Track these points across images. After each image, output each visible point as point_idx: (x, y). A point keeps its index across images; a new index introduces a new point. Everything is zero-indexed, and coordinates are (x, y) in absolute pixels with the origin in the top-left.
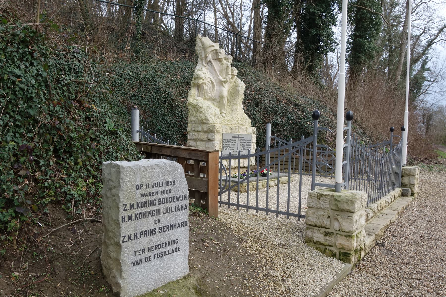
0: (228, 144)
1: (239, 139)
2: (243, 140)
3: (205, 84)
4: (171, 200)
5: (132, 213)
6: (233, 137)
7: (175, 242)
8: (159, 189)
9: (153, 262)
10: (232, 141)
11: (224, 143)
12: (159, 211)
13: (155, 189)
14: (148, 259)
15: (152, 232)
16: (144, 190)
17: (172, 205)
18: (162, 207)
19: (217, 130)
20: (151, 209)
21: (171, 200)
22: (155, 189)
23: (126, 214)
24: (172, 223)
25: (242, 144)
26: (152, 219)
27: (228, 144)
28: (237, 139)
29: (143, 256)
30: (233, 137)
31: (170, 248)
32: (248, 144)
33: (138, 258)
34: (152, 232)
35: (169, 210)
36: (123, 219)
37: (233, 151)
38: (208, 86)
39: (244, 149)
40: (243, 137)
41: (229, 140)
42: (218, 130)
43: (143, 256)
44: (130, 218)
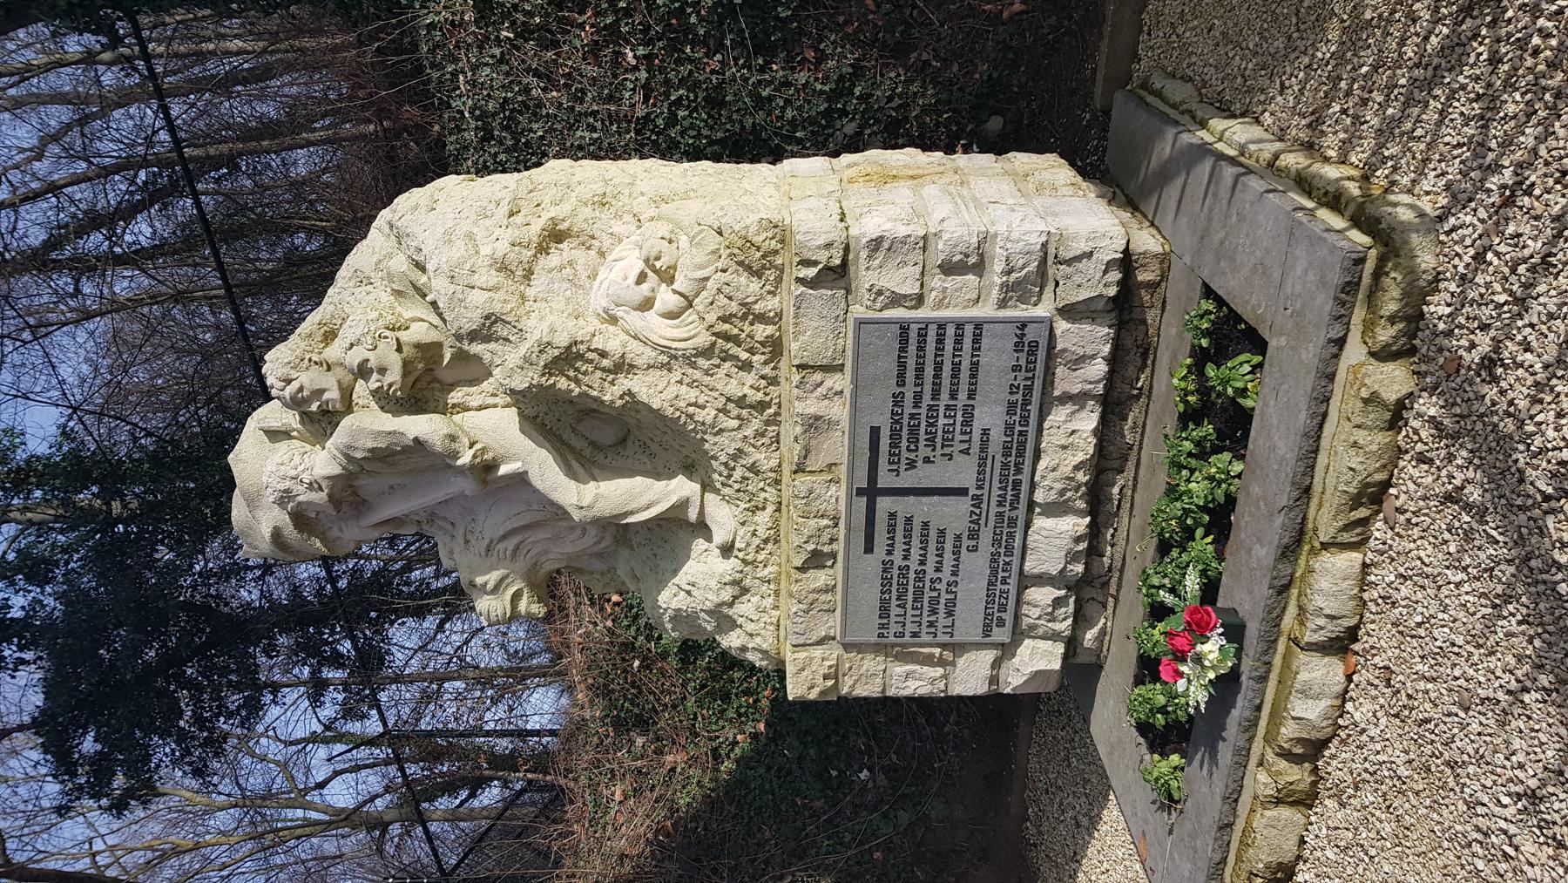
0: (918, 598)
1: (882, 483)
6: (869, 549)
11: (910, 628)
25: (924, 451)
27: (918, 598)
28: (884, 504)
30: (869, 549)
32: (929, 371)
37: (966, 542)
38: (546, 552)
39: (967, 422)
40: (875, 432)
41: (886, 583)
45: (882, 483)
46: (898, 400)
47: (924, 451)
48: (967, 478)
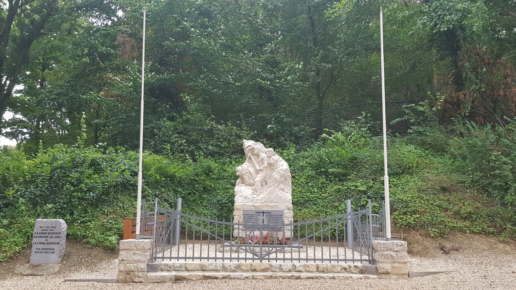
2: (271, 215)
3: (244, 174)
4: (53, 233)
5: (37, 235)
7: (53, 249)
8: (49, 229)
9: (43, 254)
10: (255, 216)
12: (48, 237)
13: (47, 229)
14: (41, 252)
15: (44, 243)
16: (43, 228)
17: (54, 236)
18: (49, 236)
19: (236, 208)
20: (44, 235)
21: (53, 233)
22: (47, 229)
23: (35, 235)
24: (53, 242)
26: (45, 239)
29: (39, 251)
31: (51, 251)
33: (37, 251)
34: (44, 243)
35: (52, 237)
36: (34, 237)
41: (252, 215)
42: (237, 208)
43: (39, 251)
44: (36, 237)
45: (265, 214)
46: (274, 215)
47: (268, 218)
48: (264, 223)
